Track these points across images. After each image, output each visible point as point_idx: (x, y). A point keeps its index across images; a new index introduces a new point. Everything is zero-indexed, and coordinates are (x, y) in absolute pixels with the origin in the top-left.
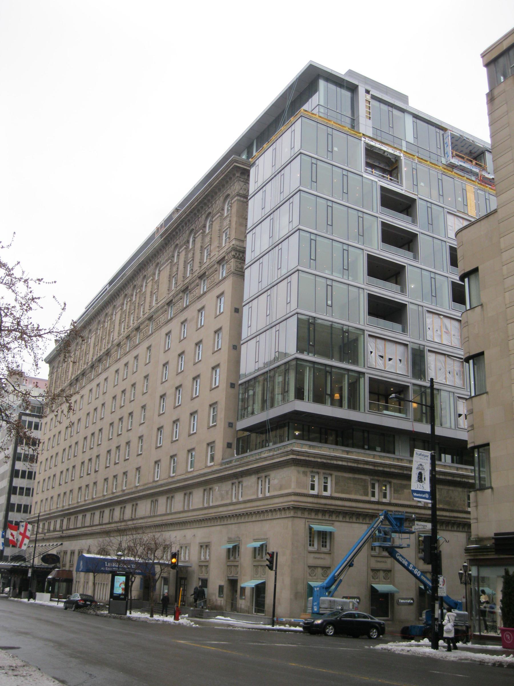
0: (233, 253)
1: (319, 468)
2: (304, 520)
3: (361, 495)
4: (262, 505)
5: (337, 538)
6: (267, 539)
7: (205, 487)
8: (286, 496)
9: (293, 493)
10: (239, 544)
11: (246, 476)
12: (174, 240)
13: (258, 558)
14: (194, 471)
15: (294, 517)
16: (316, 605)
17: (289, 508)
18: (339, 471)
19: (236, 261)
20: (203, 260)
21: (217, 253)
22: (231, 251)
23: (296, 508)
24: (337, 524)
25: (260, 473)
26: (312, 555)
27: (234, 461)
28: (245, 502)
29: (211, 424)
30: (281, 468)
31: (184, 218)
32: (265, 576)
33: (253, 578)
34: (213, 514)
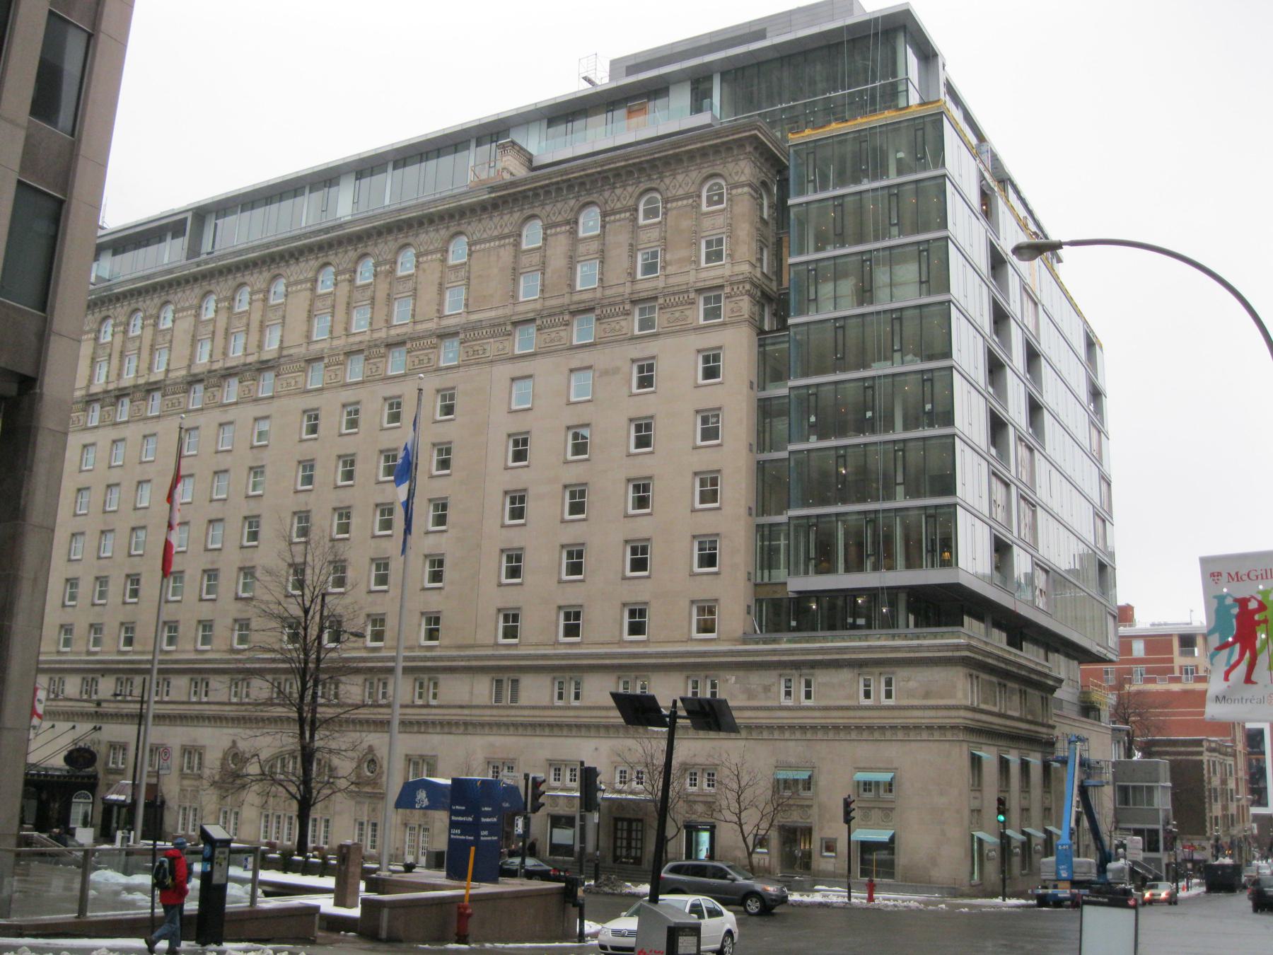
4: (876, 719)
17: (952, 728)
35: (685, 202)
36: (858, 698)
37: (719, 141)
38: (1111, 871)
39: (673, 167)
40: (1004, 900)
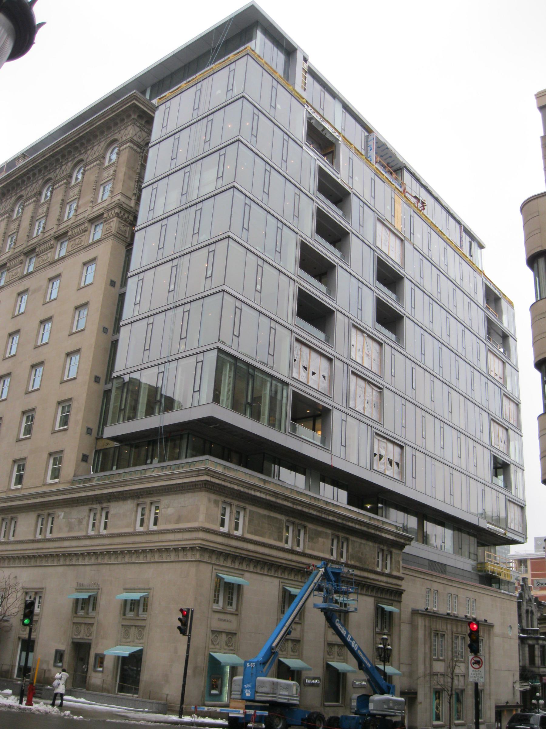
0: (117, 210)
1: (232, 499)
2: (210, 567)
3: (275, 540)
4: (142, 543)
5: (248, 595)
6: (43, 589)
7: (39, 512)
8: (189, 531)
9: (202, 527)
10: (97, 594)
11: (115, 501)
12: (16, 190)
13: (130, 615)
14: (22, 488)
15: (200, 561)
16: (248, 688)
17: (192, 549)
18: (254, 505)
19: (119, 221)
20: (33, 233)
21: (89, 209)
22: (114, 208)
23: (203, 550)
24: (247, 575)
25: (142, 498)
26: (217, 616)
27: (96, 479)
28: (112, 536)
29: (57, 428)
30: (182, 493)
31: (39, 163)
32: (141, 641)
33: (119, 643)
34: (53, 550)
35: (95, 163)
36: (135, 527)
37: (114, 114)
38: (373, 701)
39: (92, 142)
40: (180, 717)
